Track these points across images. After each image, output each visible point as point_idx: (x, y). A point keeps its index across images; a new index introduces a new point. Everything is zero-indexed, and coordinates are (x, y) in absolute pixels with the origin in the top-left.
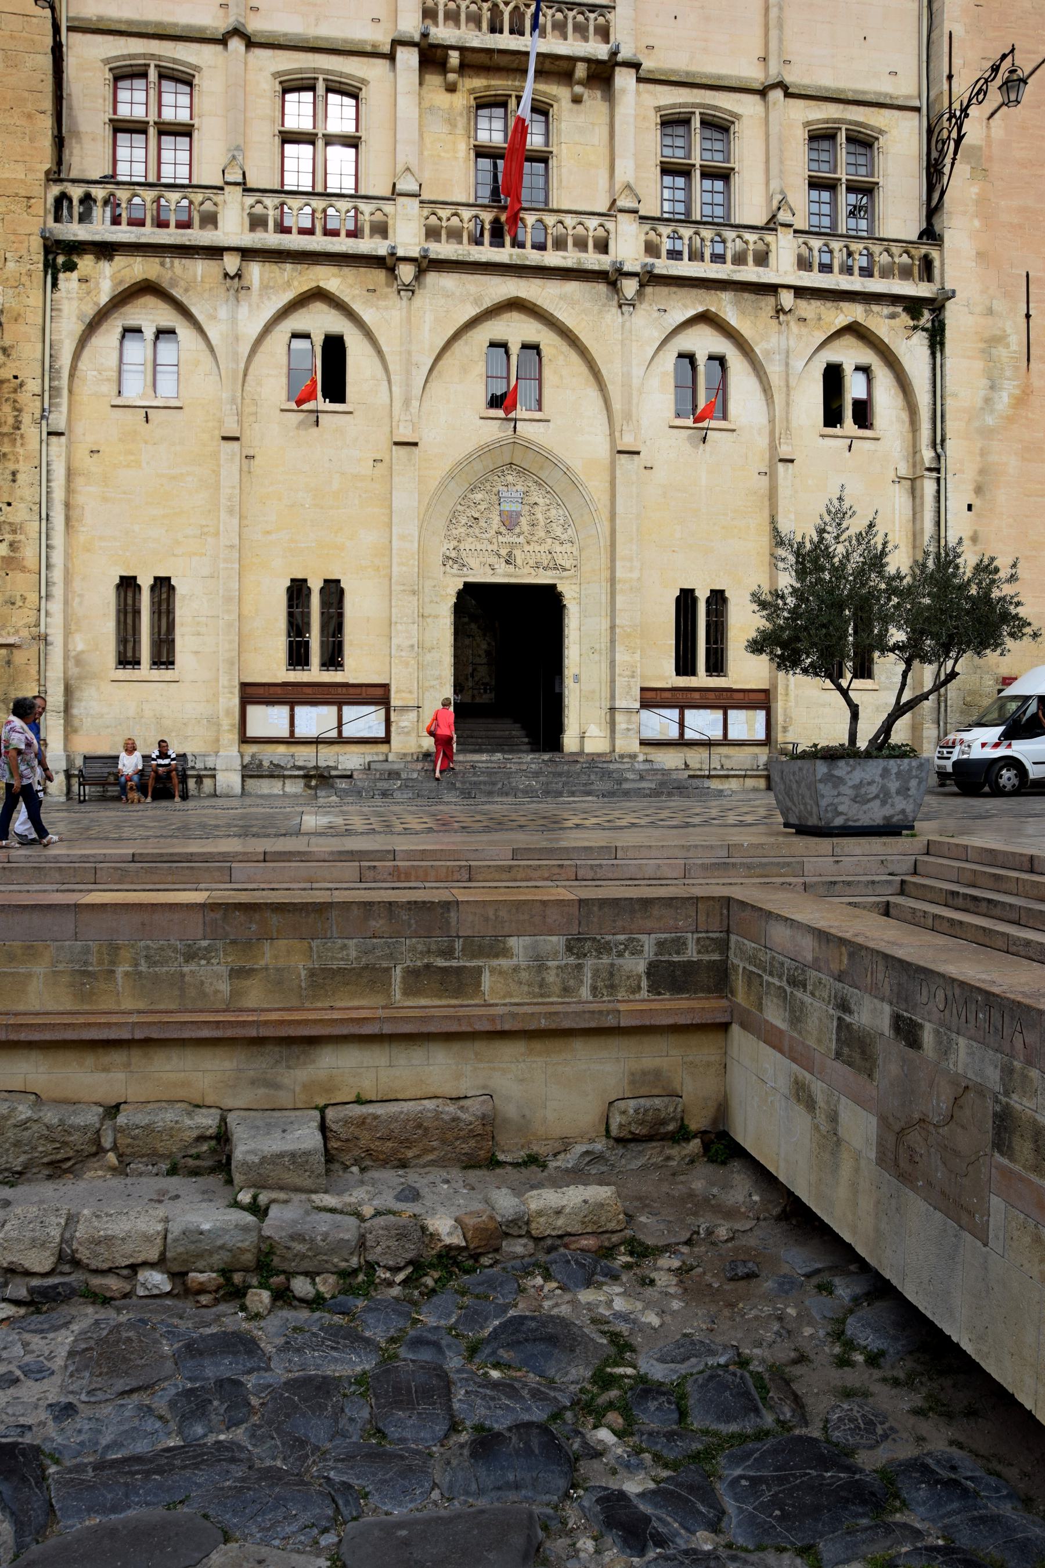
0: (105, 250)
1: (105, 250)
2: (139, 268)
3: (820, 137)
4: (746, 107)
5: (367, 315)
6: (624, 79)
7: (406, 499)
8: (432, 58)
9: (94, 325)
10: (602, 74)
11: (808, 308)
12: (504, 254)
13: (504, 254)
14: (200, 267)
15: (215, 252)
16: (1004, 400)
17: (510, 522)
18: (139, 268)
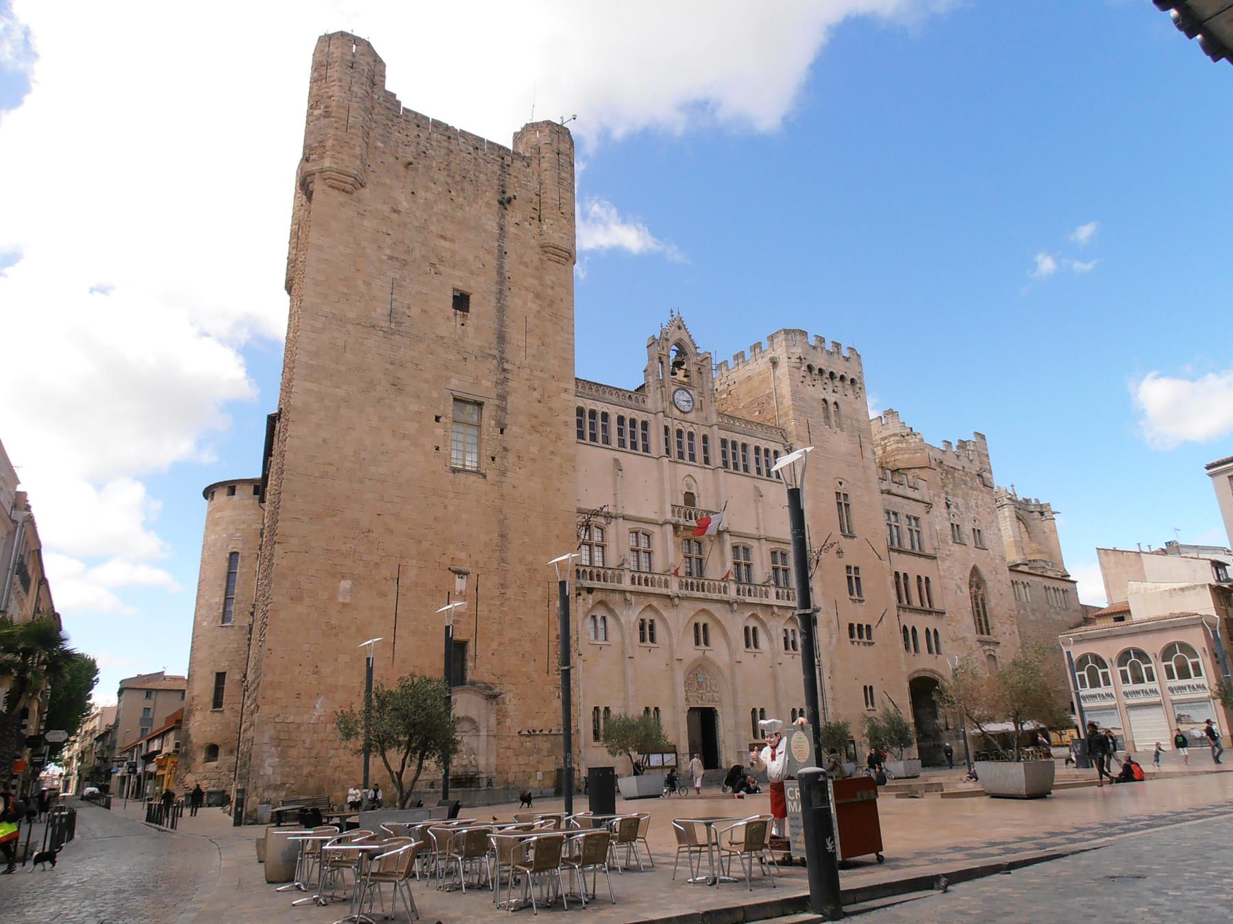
0: (590, 590)
1: (590, 590)
2: (599, 596)
3: (774, 553)
4: (754, 544)
5: (665, 614)
6: (727, 537)
7: (680, 679)
8: (676, 527)
9: (586, 615)
10: (720, 533)
11: (780, 612)
12: (700, 594)
13: (700, 594)
14: (617, 596)
15: (623, 592)
16: (834, 641)
17: (700, 685)
18: (599, 596)
